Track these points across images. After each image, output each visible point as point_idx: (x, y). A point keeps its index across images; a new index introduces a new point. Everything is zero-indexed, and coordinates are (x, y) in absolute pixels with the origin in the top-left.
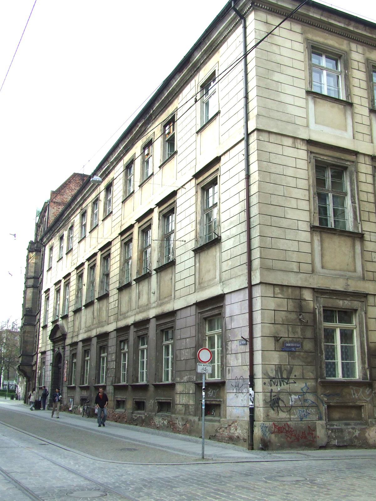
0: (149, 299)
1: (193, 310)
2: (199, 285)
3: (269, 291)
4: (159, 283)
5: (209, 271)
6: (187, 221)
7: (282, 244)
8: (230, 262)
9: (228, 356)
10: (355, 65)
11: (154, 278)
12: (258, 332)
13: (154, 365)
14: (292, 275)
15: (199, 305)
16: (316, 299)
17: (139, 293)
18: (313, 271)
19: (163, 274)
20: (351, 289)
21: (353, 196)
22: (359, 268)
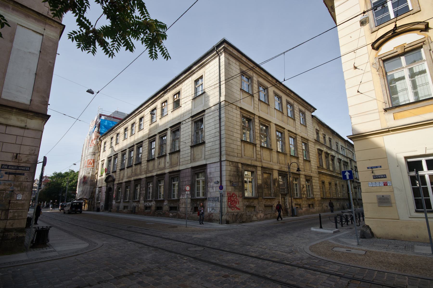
0: (165, 165)
1: (190, 170)
2: (193, 159)
3: (228, 163)
4: (170, 159)
5: (199, 155)
6: (187, 135)
7: (232, 146)
8: (210, 152)
9: (208, 188)
10: (254, 82)
11: (168, 157)
12: (224, 179)
13: (167, 192)
14: (235, 158)
15: (192, 168)
16: (242, 167)
17: (159, 163)
18: (242, 157)
19: (173, 155)
20: (253, 164)
21: (253, 130)
22: (255, 157)
